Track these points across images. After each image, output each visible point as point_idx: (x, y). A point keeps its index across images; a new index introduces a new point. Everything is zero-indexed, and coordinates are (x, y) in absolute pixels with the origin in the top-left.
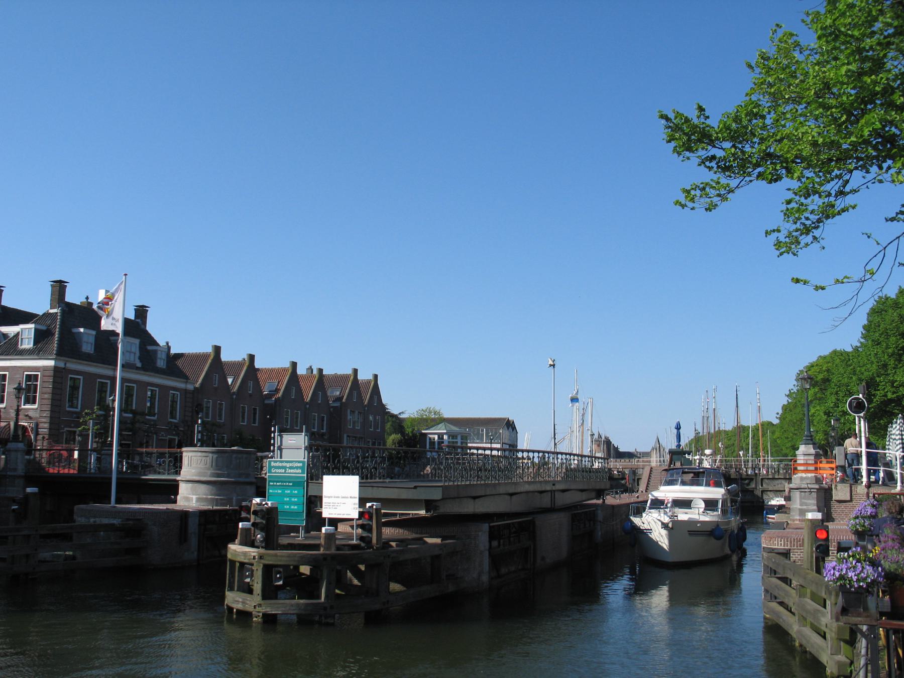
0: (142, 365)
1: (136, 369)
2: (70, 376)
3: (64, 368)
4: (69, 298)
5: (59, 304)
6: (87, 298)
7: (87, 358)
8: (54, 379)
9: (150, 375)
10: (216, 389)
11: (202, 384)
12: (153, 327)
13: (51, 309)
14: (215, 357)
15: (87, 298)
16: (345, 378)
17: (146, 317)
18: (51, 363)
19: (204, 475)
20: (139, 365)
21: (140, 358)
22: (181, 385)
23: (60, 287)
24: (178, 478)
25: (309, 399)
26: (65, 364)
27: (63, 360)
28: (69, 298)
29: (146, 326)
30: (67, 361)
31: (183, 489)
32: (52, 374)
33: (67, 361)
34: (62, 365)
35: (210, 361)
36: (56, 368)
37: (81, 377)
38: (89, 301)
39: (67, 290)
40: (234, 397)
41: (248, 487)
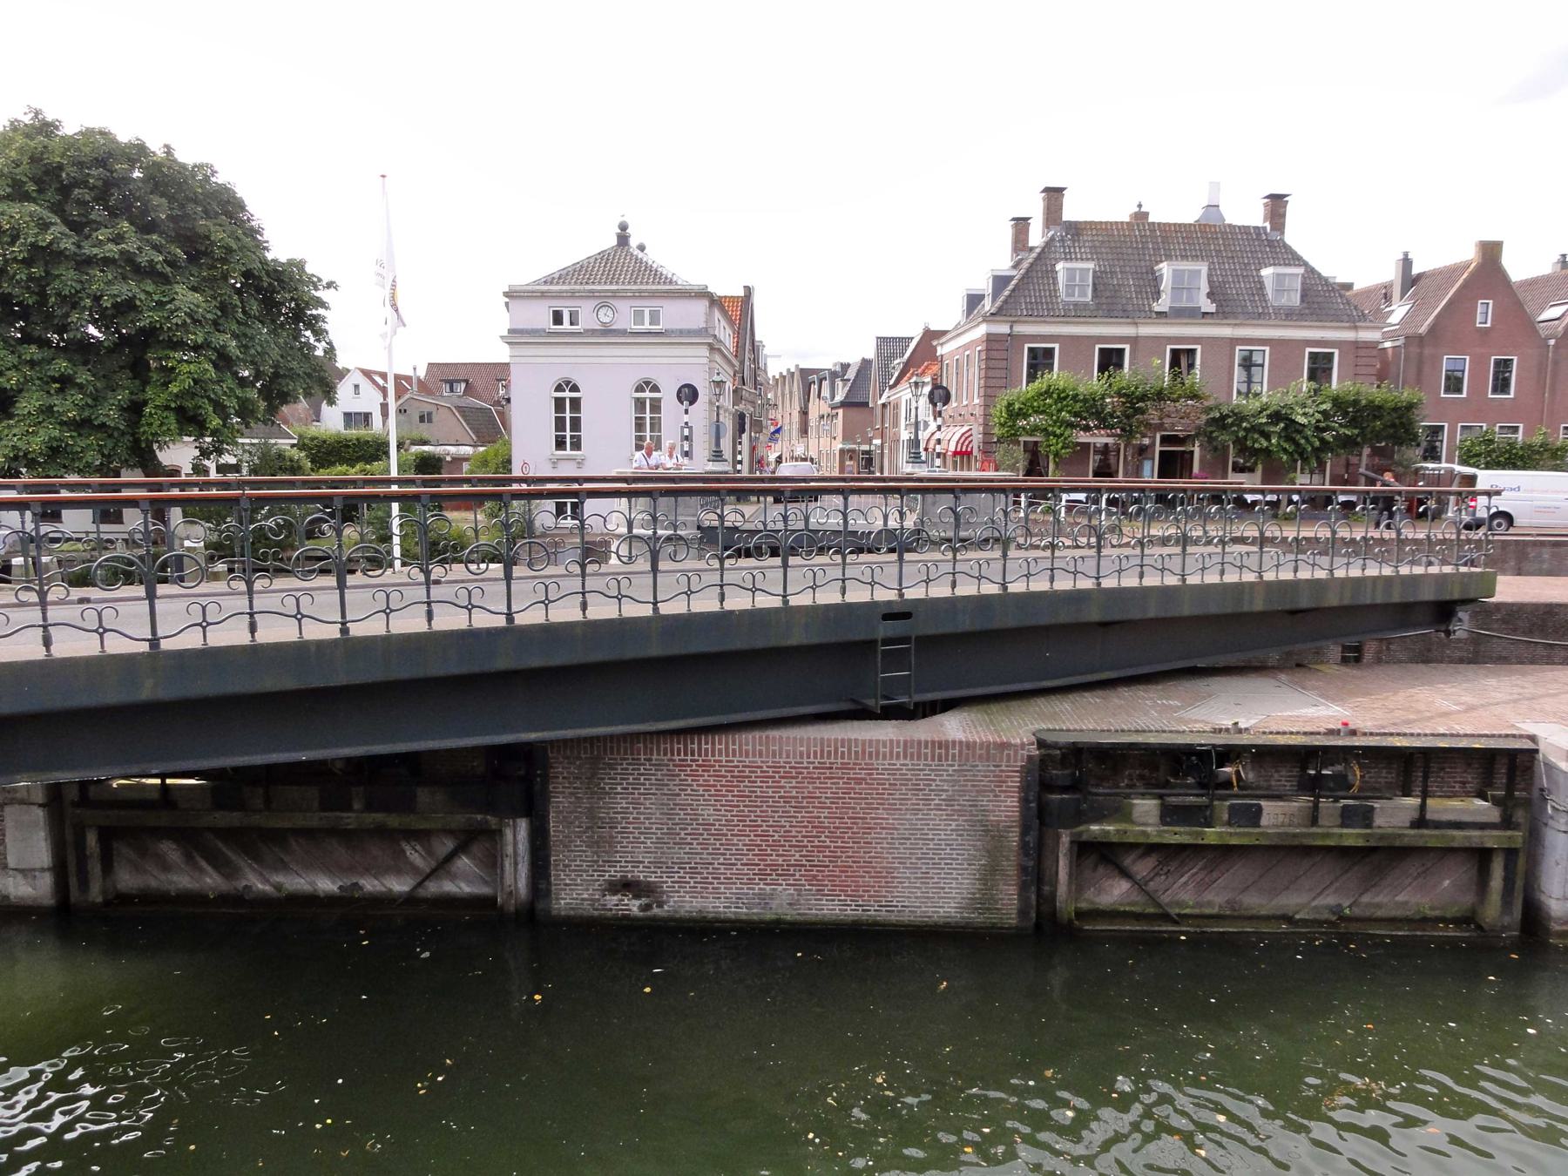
3: (1009, 335)
5: (1048, 228)
6: (1140, 206)
7: (1077, 313)
11: (1433, 329)
15: (1140, 206)
17: (1284, 216)
18: (982, 330)
20: (1212, 308)
22: (1348, 335)
23: (1054, 195)
26: (1011, 327)
27: (1007, 322)
29: (1283, 233)
34: (1004, 329)
37: (1057, 346)
38: (1143, 210)
40: (1552, 342)
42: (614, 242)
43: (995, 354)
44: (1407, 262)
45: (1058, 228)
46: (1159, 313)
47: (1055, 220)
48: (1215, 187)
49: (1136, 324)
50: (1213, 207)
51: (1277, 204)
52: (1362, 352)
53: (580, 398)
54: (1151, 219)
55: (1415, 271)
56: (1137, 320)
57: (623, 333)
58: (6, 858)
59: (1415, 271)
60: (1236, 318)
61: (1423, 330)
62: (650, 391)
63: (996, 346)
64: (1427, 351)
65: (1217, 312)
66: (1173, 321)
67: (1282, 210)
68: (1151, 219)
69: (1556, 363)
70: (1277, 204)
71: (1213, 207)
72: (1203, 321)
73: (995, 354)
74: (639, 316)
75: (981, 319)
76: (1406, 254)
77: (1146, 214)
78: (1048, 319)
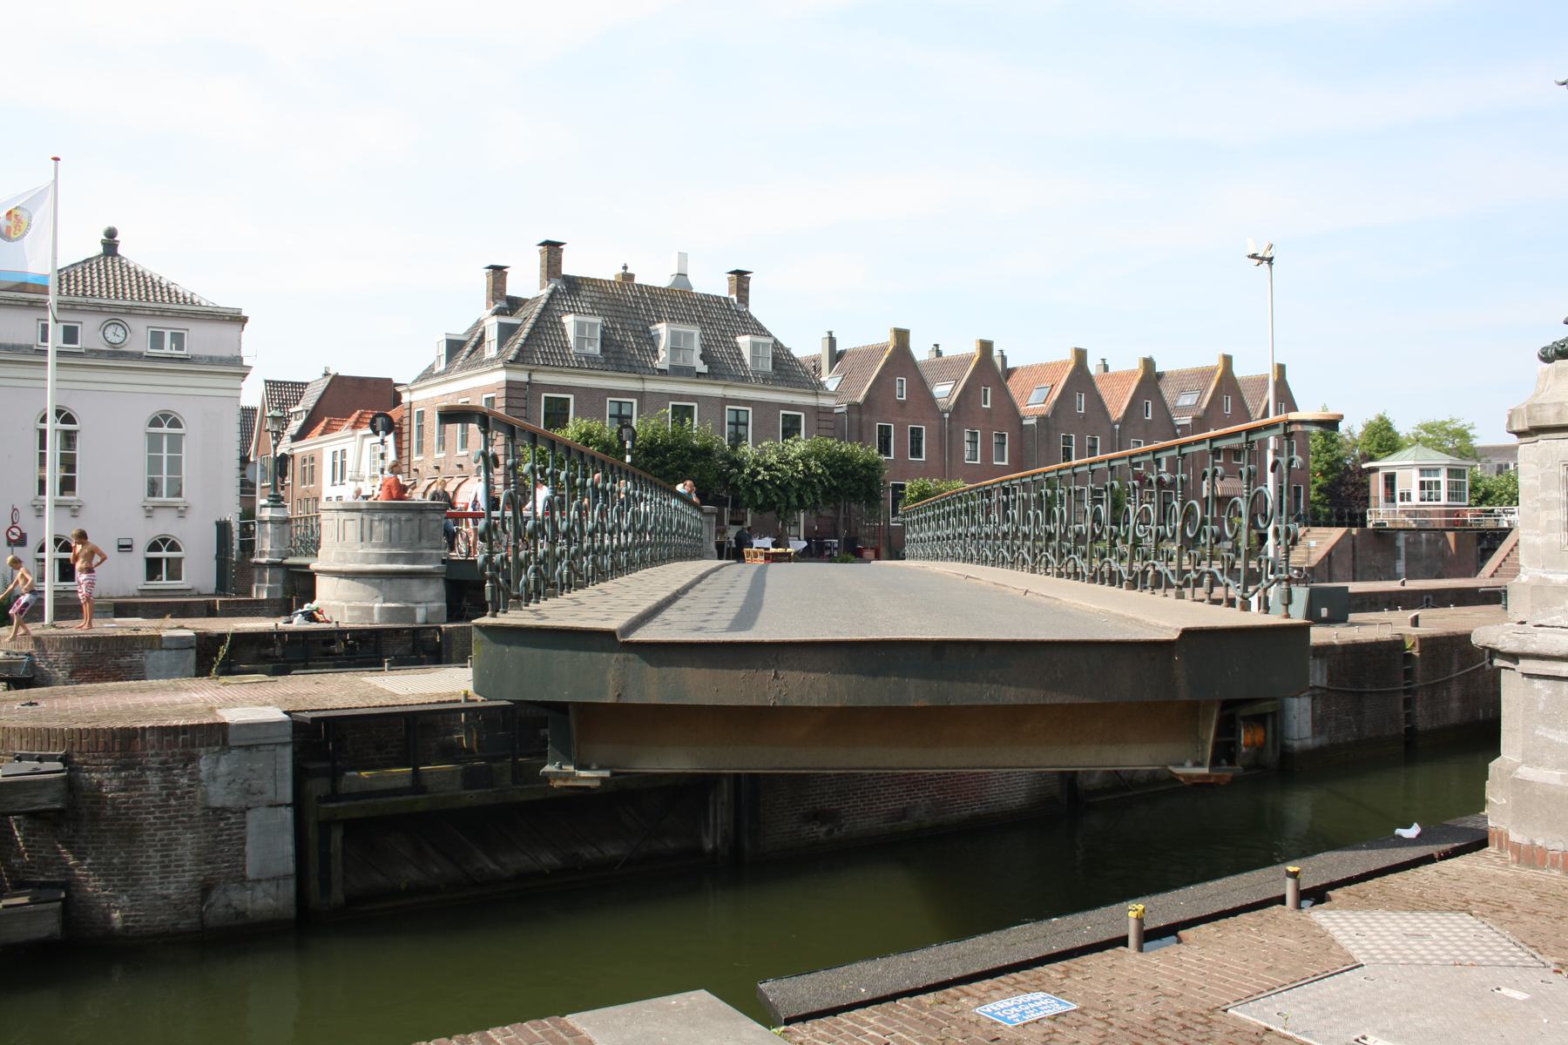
0: (710, 368)
1: (698, 377)
2: (544, 395)
3: (528, 383)
4: (567, 270)
5: (548, 280)
6: (625, 268)
8: (506, 401)
9: (726, 386)
10: (902, 404)
11: (868, 398)
12: (757, 307)
13: (541, 289)
14: (895, 350)
15: (625, 268)
16: (1205, 374)
18: (500, 377)
19: (366, 558)
20: (704, 369)
21: (702, 357)
22: (810, 401)
23: (553, 249)
24: (314, 566)
25: (1121, 414)
26: (530, 375)
27: (526, 370)
28: (567, 270)
29: (747, 306)
30: (533, 370)
31: (323, 586)
32: (504, 395)
33: (533, 370)
34: (522, 377)
35: (886, 356)
36: (510, 386)
37: (571, 397)
38: (628, 271)
39: (563, 255)
40: (947, 415)
41: (415, 584)
42: (100, 249)
43: (515, 403)
44: (832, 341)
45: (558, 281)
46: (661, 371)
47: (555, 273)
48: (683, 257)
49: (643, 379)
50: (682, 276)
51: (741, 278)
52: (822, 417)
53: (75, 432)
54: (637, 281)
55: (839, 348)
56: (644, 376)
57: (139, 356)
58: (244, 870)
59: (839, 348)
60: (725, 379)
61: (860, 399)
62: (169, 426)
63: (515, 394)
64: (865, 418)
65: (709, 373)
66: (672, 378)
67: (745, 285)
68: (637, 281)
69: (950, 432)
70: (741, 278)
71: (682, 276)
72: (697, 380)
73: (515, 403)
74: (157, 339)
75: (501, 365)
76: (830, 333)
77: (631, 277)
78: (564, 370)
